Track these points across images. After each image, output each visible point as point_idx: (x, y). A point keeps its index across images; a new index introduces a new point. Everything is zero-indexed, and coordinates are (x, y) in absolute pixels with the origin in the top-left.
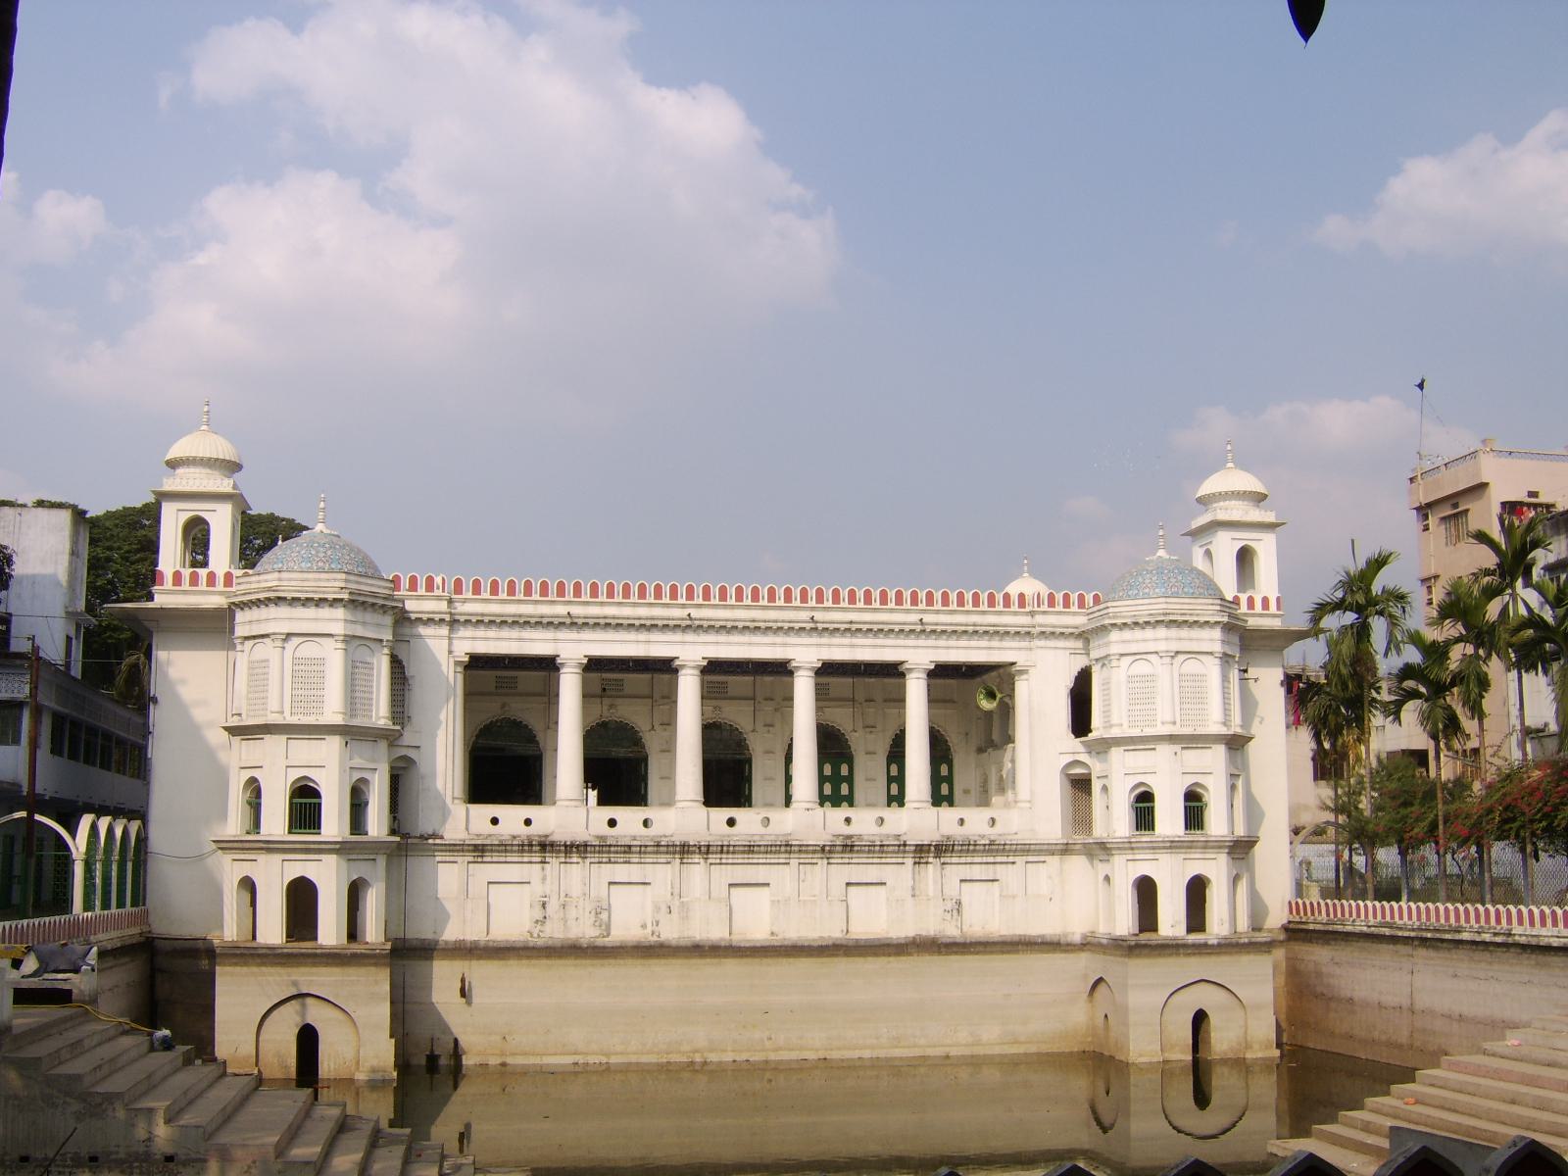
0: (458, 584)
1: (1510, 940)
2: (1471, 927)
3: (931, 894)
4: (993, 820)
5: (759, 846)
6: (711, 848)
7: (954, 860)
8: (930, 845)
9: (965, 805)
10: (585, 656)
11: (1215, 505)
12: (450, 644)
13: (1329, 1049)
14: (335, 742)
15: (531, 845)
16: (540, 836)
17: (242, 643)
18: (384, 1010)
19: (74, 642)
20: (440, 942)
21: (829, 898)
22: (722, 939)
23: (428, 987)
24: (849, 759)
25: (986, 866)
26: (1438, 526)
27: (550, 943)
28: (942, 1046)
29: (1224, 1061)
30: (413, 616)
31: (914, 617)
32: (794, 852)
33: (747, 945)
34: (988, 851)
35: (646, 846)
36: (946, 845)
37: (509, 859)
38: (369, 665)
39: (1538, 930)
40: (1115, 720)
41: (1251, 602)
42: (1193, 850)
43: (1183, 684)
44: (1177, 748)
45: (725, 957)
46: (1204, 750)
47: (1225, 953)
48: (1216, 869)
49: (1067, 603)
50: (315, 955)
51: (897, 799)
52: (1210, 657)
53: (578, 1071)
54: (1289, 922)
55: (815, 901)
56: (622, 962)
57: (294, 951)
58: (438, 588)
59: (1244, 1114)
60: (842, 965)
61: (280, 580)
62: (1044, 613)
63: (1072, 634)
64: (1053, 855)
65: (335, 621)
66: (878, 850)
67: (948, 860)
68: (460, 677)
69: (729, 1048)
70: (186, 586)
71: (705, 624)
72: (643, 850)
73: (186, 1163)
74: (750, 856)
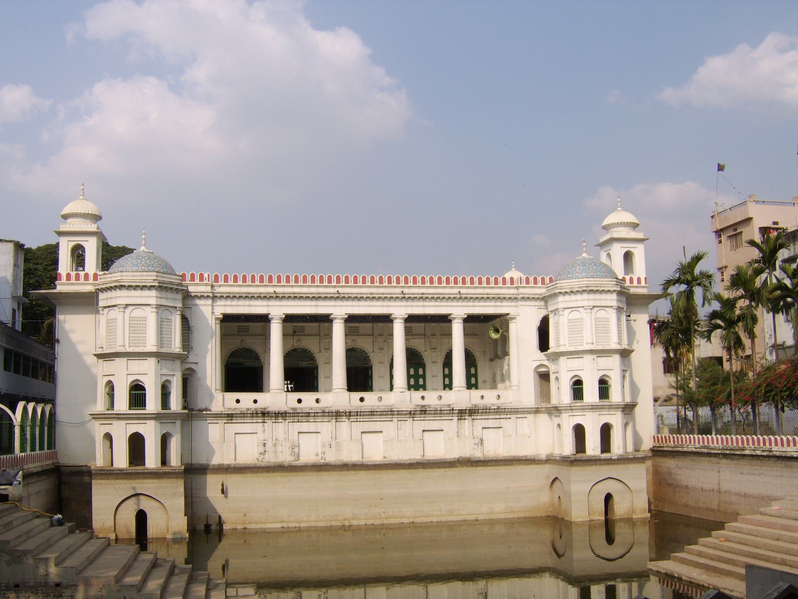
0: (216, 277)
1: (771, 454)
2: (750, 447)
3: (467, 435)
4: (499, 396)
5: (377, 411)
6: (351, 413)
7: (479, 417)
8: (466, 410)
9: (485, 389)
10: (284, 314)
11: (612, 230)
12: (213, 309)
13: (676, 512)
14: (152, 361)
15: (257, 413)
16: (262, 409)
17: (103, 310)
18: (181, 502)
19: (17, 311)
20: (211, 465)
21: (414, 438)
22: (358, 461)
23: (204, 488)
24: (423, 366)
25: (496, 420)
26: (727, 240)
27: (268, 464)
28: (474, 514)
29: (622, 520)
30: (193, 294)
31: (456, 291)
32: (395, 415)
33: (371, 463)
34: (496, 412)
35: (317, 413)
36: (474, 410)
37: (245, 421)
38: (170, 321)
39: (786, 448)
40: (561, 343)
41: (631, 280)
42: (604, 410)
43: (597, 323)
44: (595, 356)
45: (360, 470)
46: (608, 358)
47: (621, 463)
48: (616, 420)
49: (535, 282)
50: (144, 473)
51: (449, 386)
52: (611, 309)
53: (284, 531)
54: (654, 447)
55: (407, 440)
56: (306, 473)
57: (133, 471)
58: (206, 280)
59: (632, 547)
60: (421, 473)
61: (121, 276)
62: (524, 287)
63: (538, 298)
64: (530, 413)
65: (151, 297)
66: (439, 413)
67: (475, 417)
68: (218, 326)
69: (363, 518)
70: (73, 281)
71: (346, 296)
72: (316, 415)
73: (67, 587)
74: (372, 417)
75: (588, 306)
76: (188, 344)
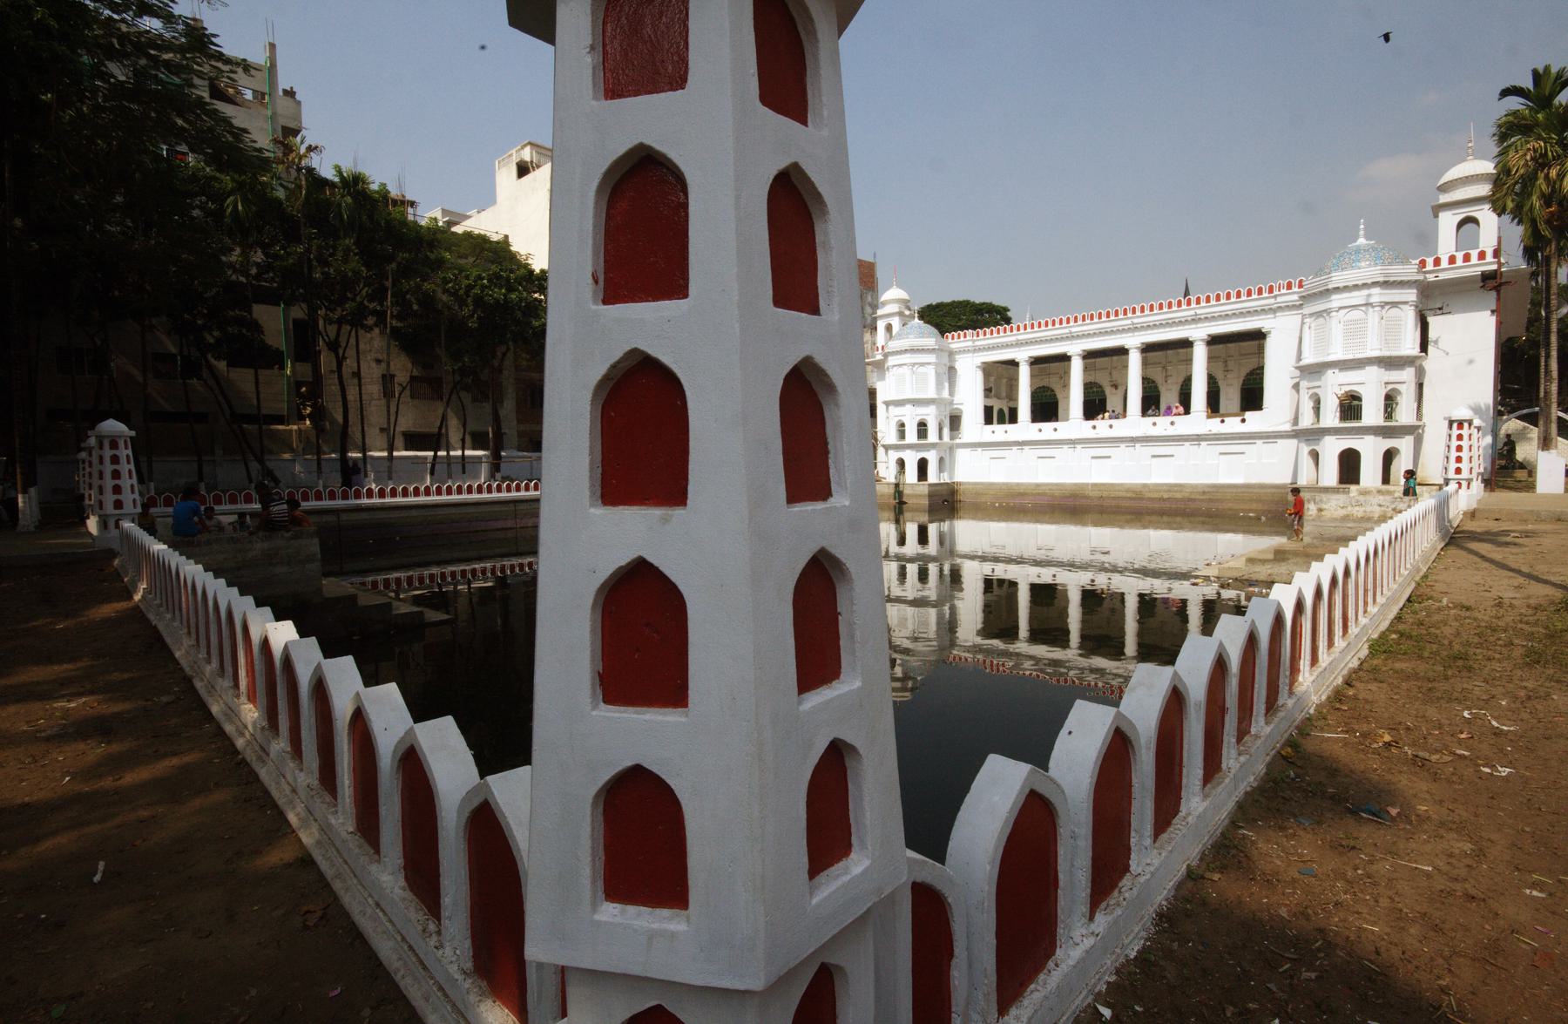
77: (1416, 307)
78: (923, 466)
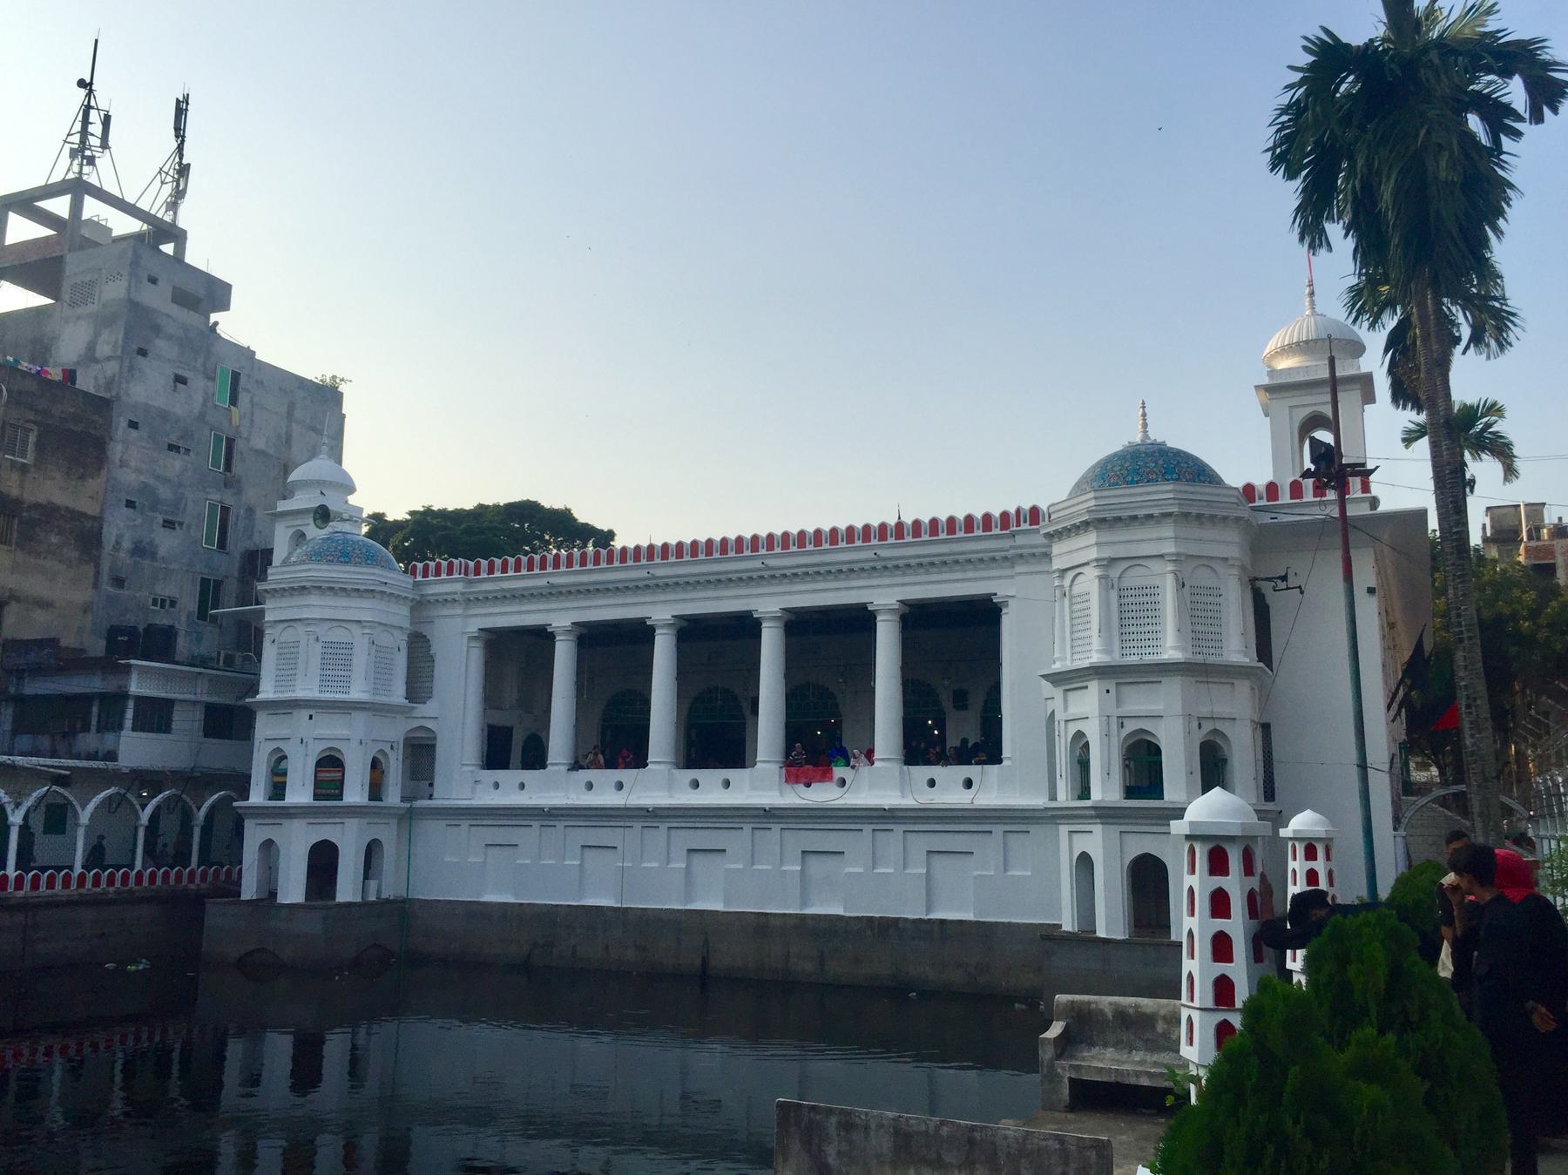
30: (432, 599)
43: (1123, 601)
75: (1097, 560)
76: (428, 684)
77: (1243, 568)
78: (323, 861)
